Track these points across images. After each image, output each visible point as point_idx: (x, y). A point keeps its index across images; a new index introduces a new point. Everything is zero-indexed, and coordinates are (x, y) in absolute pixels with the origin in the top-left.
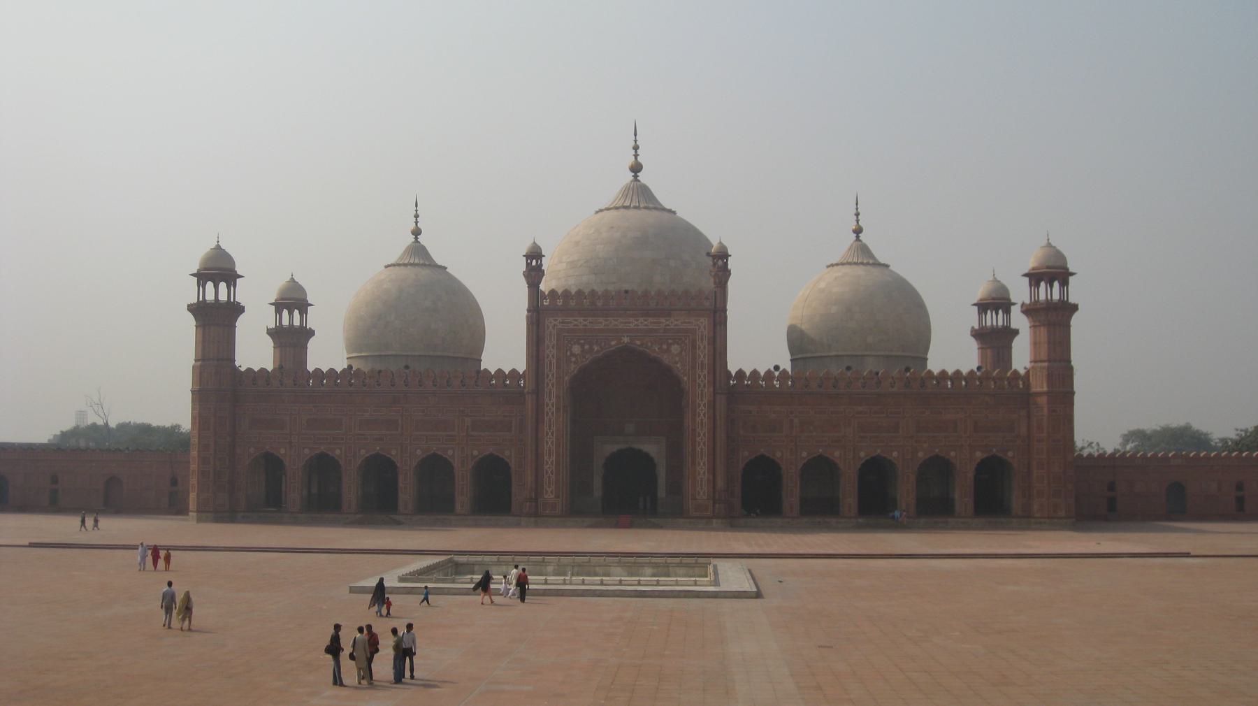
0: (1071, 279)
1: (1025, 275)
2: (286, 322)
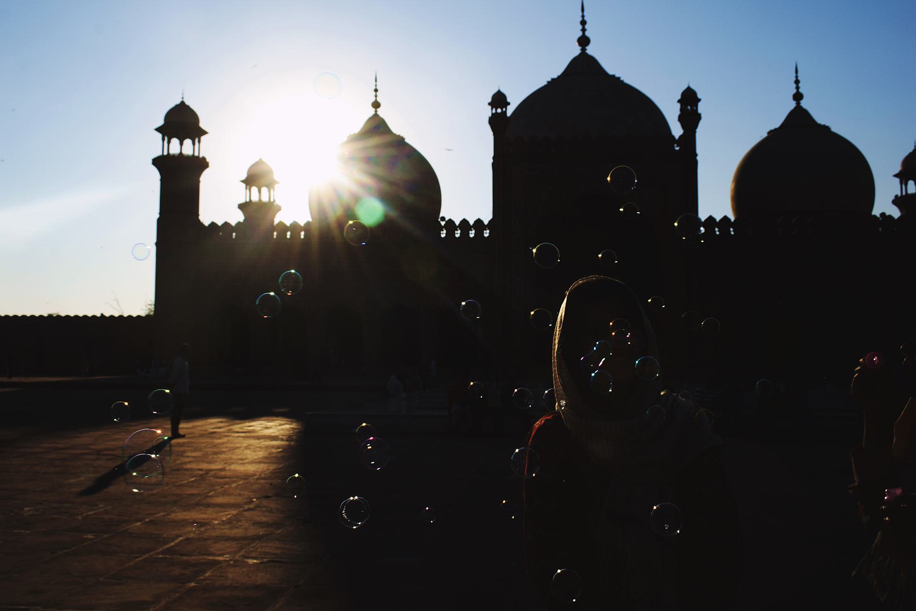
2: (255, 198)
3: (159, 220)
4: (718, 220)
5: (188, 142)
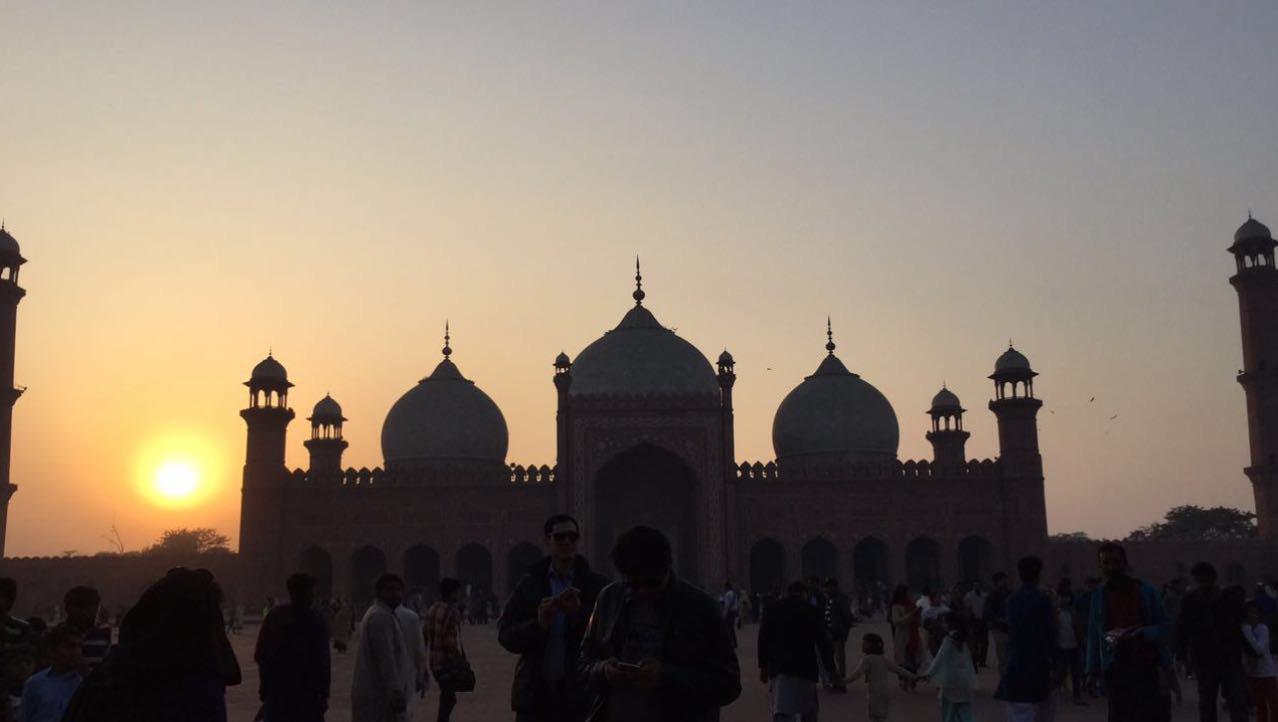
0: (1034, 379)
1: (990, 377)
2: (321, 436)
3: (246, 468)
4: (752, 465)
5: (274, 394)
